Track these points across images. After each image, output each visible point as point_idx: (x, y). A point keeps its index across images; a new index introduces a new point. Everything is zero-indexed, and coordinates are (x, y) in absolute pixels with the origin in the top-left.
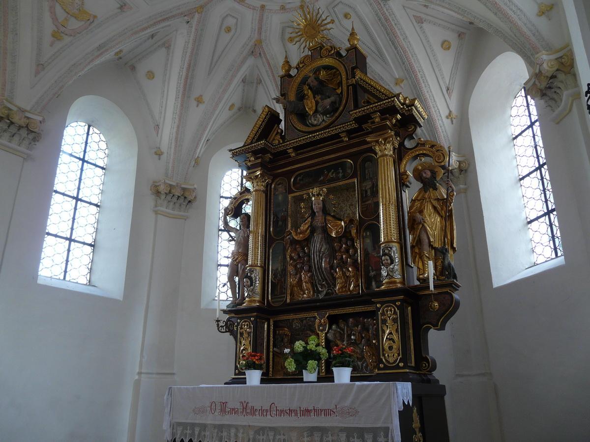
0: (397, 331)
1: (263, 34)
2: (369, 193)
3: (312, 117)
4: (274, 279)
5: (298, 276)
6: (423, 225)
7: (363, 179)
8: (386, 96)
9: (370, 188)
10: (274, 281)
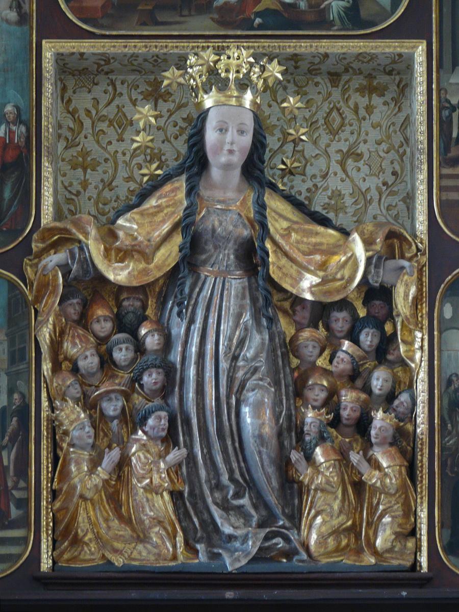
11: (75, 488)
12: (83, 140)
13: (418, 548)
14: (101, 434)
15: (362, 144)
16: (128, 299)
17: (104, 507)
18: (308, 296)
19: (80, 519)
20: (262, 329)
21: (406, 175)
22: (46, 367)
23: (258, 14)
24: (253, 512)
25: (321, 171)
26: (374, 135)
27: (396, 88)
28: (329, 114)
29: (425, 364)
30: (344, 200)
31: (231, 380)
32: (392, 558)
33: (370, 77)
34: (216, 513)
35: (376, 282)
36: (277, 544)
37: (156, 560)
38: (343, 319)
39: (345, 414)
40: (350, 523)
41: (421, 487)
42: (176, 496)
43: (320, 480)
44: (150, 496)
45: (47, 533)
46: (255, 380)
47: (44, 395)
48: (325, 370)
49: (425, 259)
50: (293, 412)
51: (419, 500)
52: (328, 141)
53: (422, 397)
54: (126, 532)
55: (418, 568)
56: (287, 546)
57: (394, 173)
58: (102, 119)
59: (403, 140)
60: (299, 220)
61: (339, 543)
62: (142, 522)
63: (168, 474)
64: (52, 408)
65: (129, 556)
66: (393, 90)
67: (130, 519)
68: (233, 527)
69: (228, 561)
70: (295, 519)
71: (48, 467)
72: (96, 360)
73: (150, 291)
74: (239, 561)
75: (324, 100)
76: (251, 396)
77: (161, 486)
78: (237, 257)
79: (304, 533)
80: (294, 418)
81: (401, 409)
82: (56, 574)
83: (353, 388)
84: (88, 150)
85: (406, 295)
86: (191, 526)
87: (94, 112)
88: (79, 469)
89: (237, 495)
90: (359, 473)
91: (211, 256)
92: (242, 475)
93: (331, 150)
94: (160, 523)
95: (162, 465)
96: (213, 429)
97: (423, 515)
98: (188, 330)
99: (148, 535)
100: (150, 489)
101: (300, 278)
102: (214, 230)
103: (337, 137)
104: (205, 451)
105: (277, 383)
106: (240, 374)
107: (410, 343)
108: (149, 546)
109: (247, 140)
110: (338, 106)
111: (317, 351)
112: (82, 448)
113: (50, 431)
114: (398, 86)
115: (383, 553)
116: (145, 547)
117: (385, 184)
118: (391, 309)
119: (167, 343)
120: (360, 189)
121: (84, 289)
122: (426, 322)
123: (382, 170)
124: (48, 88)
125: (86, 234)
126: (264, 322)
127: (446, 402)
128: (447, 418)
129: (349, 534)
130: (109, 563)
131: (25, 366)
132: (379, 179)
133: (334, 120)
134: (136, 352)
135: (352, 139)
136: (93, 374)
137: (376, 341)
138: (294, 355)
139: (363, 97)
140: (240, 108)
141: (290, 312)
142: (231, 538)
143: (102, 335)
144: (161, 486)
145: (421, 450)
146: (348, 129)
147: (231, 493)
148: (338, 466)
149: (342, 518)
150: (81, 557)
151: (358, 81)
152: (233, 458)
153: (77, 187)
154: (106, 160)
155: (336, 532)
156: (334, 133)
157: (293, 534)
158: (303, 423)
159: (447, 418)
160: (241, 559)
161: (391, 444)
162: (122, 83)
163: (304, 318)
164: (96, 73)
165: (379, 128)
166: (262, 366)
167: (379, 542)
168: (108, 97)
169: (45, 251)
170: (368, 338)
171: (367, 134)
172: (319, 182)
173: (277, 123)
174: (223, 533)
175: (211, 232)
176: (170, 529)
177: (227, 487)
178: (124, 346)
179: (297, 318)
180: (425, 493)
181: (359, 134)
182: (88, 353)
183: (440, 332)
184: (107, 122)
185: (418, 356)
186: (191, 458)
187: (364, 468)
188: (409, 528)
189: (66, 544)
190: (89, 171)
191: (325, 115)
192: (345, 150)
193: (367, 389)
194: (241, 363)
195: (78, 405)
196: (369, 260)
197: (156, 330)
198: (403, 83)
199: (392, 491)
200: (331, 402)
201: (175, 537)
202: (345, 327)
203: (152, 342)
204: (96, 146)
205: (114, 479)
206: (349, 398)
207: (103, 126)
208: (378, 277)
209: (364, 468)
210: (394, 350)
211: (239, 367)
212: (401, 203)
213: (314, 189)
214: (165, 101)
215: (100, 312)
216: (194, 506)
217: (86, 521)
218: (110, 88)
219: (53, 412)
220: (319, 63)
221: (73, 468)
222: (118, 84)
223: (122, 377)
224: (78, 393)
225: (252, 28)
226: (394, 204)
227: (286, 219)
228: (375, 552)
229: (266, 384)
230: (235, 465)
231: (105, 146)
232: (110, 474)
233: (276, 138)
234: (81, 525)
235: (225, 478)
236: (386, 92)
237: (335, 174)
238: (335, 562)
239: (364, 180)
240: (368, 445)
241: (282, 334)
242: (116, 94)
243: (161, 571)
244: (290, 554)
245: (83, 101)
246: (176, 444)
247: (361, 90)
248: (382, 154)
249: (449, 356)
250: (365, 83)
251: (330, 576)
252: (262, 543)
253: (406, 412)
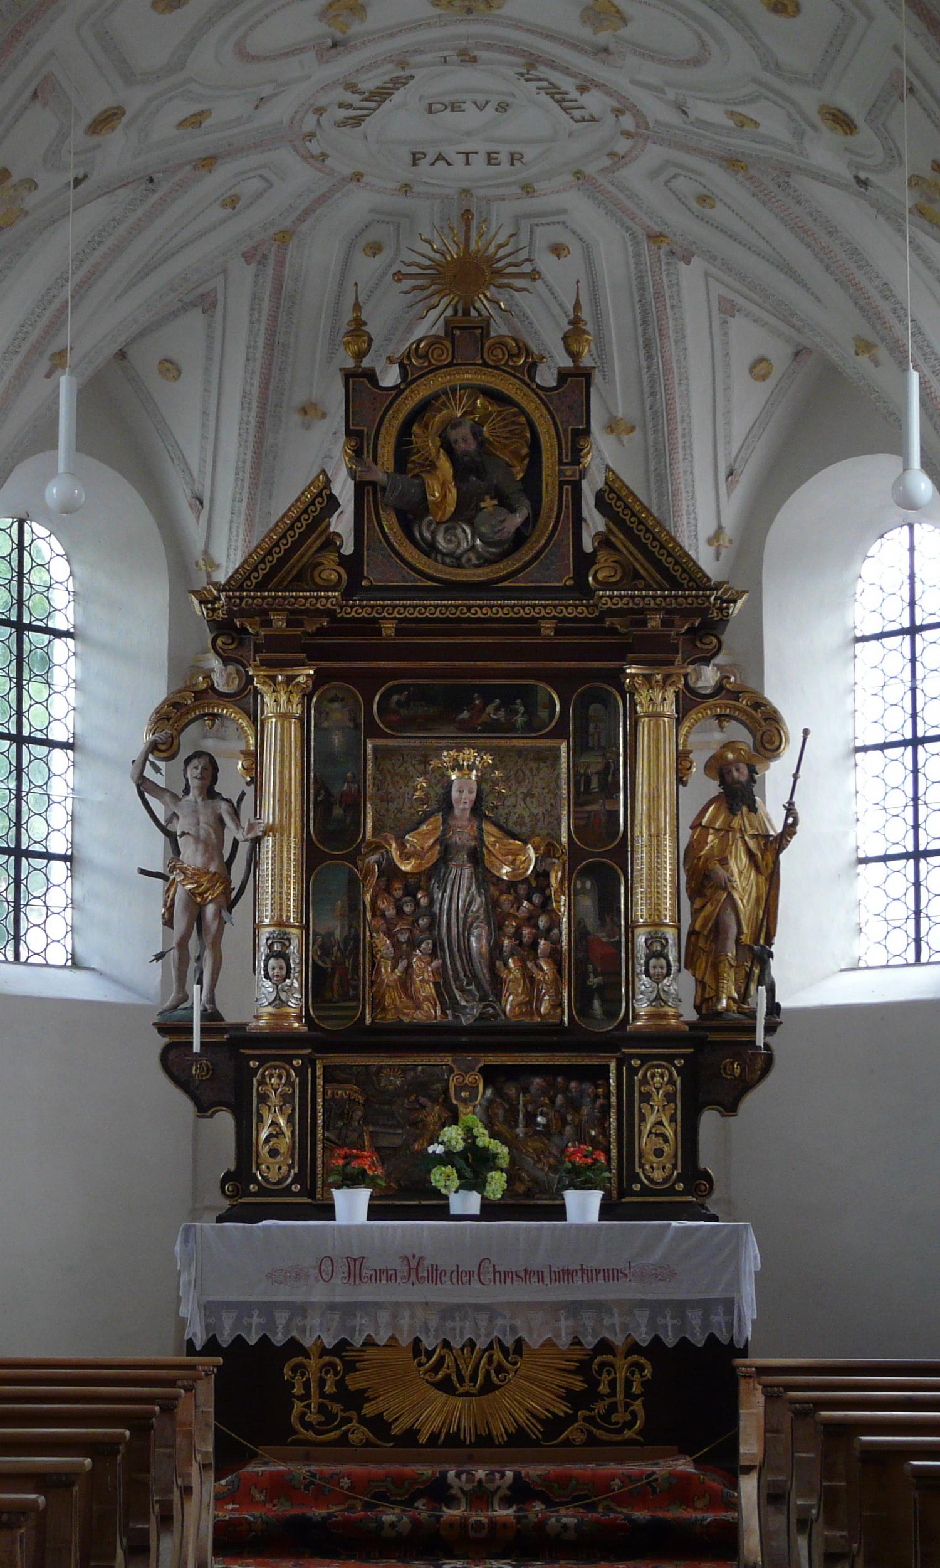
0: (673, 1119)
1: (304, 227)
2: (595, 784)
3: (442, 528)
4: (320, 957)
5: (402, 964)
6: (729, 894)
7: (580, 748)
8: (691, 579)
9: (598, 773)
10: (320, 963)
11: (383, 981)
13: (563, 1012)
18: (505, 878)
22: (369, 916)
23: (479, 725)
29: (566, 913)
34: (457, 993)
39: (525, 940)
42: (436, 984)
43: (511, 976)
47: (367, 929)
49: (566, 858)
53: (565, 931)
54: (411, 1004)
64: (372, 937)
70: (498, 996)
76: (475, 932)
78: (468, 857)
79: (503, 1004)
83: (529, 926)
85: (556, 877)
88: (386, 971)
89: (468, 984)
94: (428, 1000)
95: (429, 969)
96: (456, 949)
97: (566, 995)
98: (443, 896)
100: (422, 981)
101: (502, 867)
105: (489, 924)
106: (469, 920)
107: (558, 902)
109: (474, 795)
112: (387, 959)
119: (432, 901)
122: (567, 891)
124: (370, 765)
125: (390, 845)
130: (401, 1020)
137: (541, 900)
140: (468, 151)
142: (465, 1007)
155: (519, 1005)
158: (503, 946)
161: (548, 957)
167: (542, 1010)
169: (366, 855)
170: (536, 899)
180: (566, 983)
183: (575, 895)
185: (563, 909)
186: (444, 963)
187: (535, 970)
188: (558, 1002)
193: (536, 926)
194: (470, 914)
196: (537, 858)
200: (517, 935)
203: (424, 901)
206: (526, 931)
209: (535, 970)
215: (397, 886)
221: (383, 970)
225: (475, 731)
227: (493, 836)
230: (467, 968)
235: (462, 975)
240: (536, 958)
242: (404, 761)
244: (495, 1016)
245: (387, 765)
246: (436, 957)
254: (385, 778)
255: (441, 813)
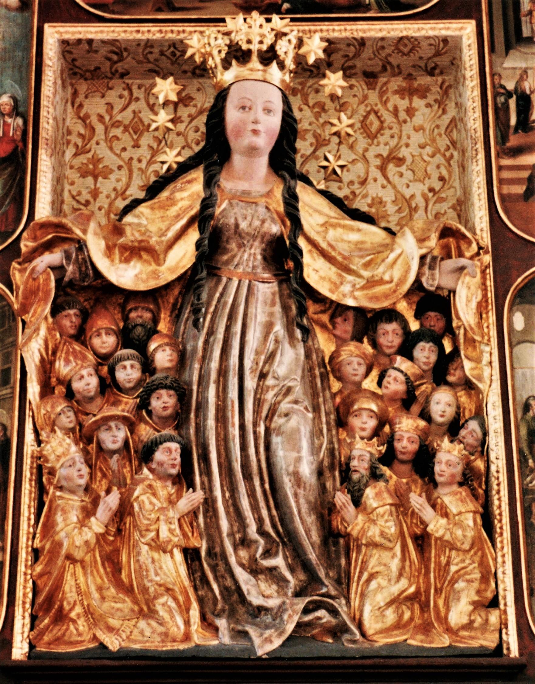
12: (94, 146)
14: (99, 474)
15: (404, 149)
16: (136, 309)
17: (98, 571)
19: (67, 588)
20: (295, 342)
21: (454, 180)
24: (288, 575)
25: (359, 177)
26: (417, 138)
27: (439, 89)
28: (366, 117)
30: (386, 208)
31: (258, 403)
32: (471, 638)
33: (410, 77)
34: (241, 575)
35: (432, 286)
36: (320, 618)
37: (163, 641)
38: (393, 331)
40: (412, 589)
41: (502, 542)
44: (156, 555)
45: (24, 607)
46: (290, 402)
48: (374, 394)
50: (336, 446)
51: (500, 560)
52: (366, 146)
54: (127, 604)
55: (505, 652)
56: (334, 621)
57: (442, 179)
58: (116, 124)
59: (449, 143)
60: (337, 216)
61: (401, 616)
62: (145, 590)
63: (181, 526)
64: (39, 442)
65: (128, 637)
66: (435, 93)
67: (132, 586)
68: (263, 596)
69: (257, 641)
71: (29, 519)
72: (94, 381)
73: (163, 302)
74: (271, 642)
75: (361, 103)
77: (170, 541)
78: (265, 258)
79: (355, 602)
80: (337, 453)
81: (470, 440)
82: (32, 662)
84: (101, 156)
86: (210, 595)
87: (107, 118)
89: (267, 554)
90: (422, 522)
91: (234, 256)
92: (274, 526)
93: (370, 155)
96: (237, 467)
99: (152, 607)
102: (237, 226)
103: (375, 141)
104: (227, 495)
105: (316, 409)
106: (270, 396)
108: (153, 623)
110: (376, 109)
111: (362, 370)
113: (35, 471)
114: (441, 87)
115: (459, 630)
116: (148, 624)
117: (431, 190)
118: (449, 321)
120: (403, 196)
121: (86, 300)
123: (427, 175)
126: (298, 333)
127: (524, 432)
128: (526, 451)
129: (412, 604)
131: (9, 391)
132: (424, 185)
133: (371, 124)
134: (144, 372)
135: (393, 143)
136: (91, 399)
138: (335, 377)
139: (403, 99)
141: (330, 326)
143: (104, 351)
144: (170, 541)
145: (498, 492)
146: (387, 132)
147: (260, 551)
148: (395, 514)
149: (404, 583)
150: (66, 638)
151: (396, 83)
152: (262, 504)
153: (86, 196)
154: (120, 168)
156: (372, 137)
157: (341, 605)
159: (526, 451)
160: (273, 639)
161: (461, 484)
162: (139, 87)
163: (346, 332)
164: (109, 75)
165: (422, 131)
166: (297, 386)
168: (123, 102)
171: (409, 138)
172: (358, 189)
173: (310, 128)
174: (250, 604)
175: (233, 227)
176: (181, 599)
177: (256, 542)
178: (128, 363)
179: (338, 332)
180: (508, 550)
181: (400, 138)
182: (84, 372)
183: (511, 346)
184: (121, 128)
187: (428, 513)
188: (489, 595)
189: (46, 621)
190: (100, 179)
191: (362, 119)
192: (385, 154)
193: (425, 415)
194: (270, 382)
195: (69, 437)
197: (167, 344)
198: (447, 84)
199: (466, 546)
201: (188, 610)
202: (397, 341)
204: (109, 152)
205: (112, 533)
207: (118, 132)
208: (434, 280)
209: (428, 513)
210: (455, 370)
211: (268, 387)
212: (451, 210)
213: (351, 197)
214: (186, 106)
216: (214, 569)
217: (74, 589)
218: (126, 93)
219: (39, 445)
220: (354, 57)
222: (135, 88)
223: (126, 403)
224: (71, 422)
226: (442, 212)
228: (449, 630)
229: (302, 409)
230: (264, 513)
231: (118, 152)
232: (106, 526)
233: (307, 143)
234: (68, 595)
235: (252, 529)
236: (428, 94)
237: (375, 180)
238: (395, 645)
239: (408, 186)
241: (319, 351)
243: (171, 656)
246: (191, 485)
247: (401, 92)
248: (427, 158)
249: (524, 375)
250: (404, 85)
251: (392, 662)
252: (300, 618)
253: (475, 443)
254: (93, 130)
255: (201, 168)
